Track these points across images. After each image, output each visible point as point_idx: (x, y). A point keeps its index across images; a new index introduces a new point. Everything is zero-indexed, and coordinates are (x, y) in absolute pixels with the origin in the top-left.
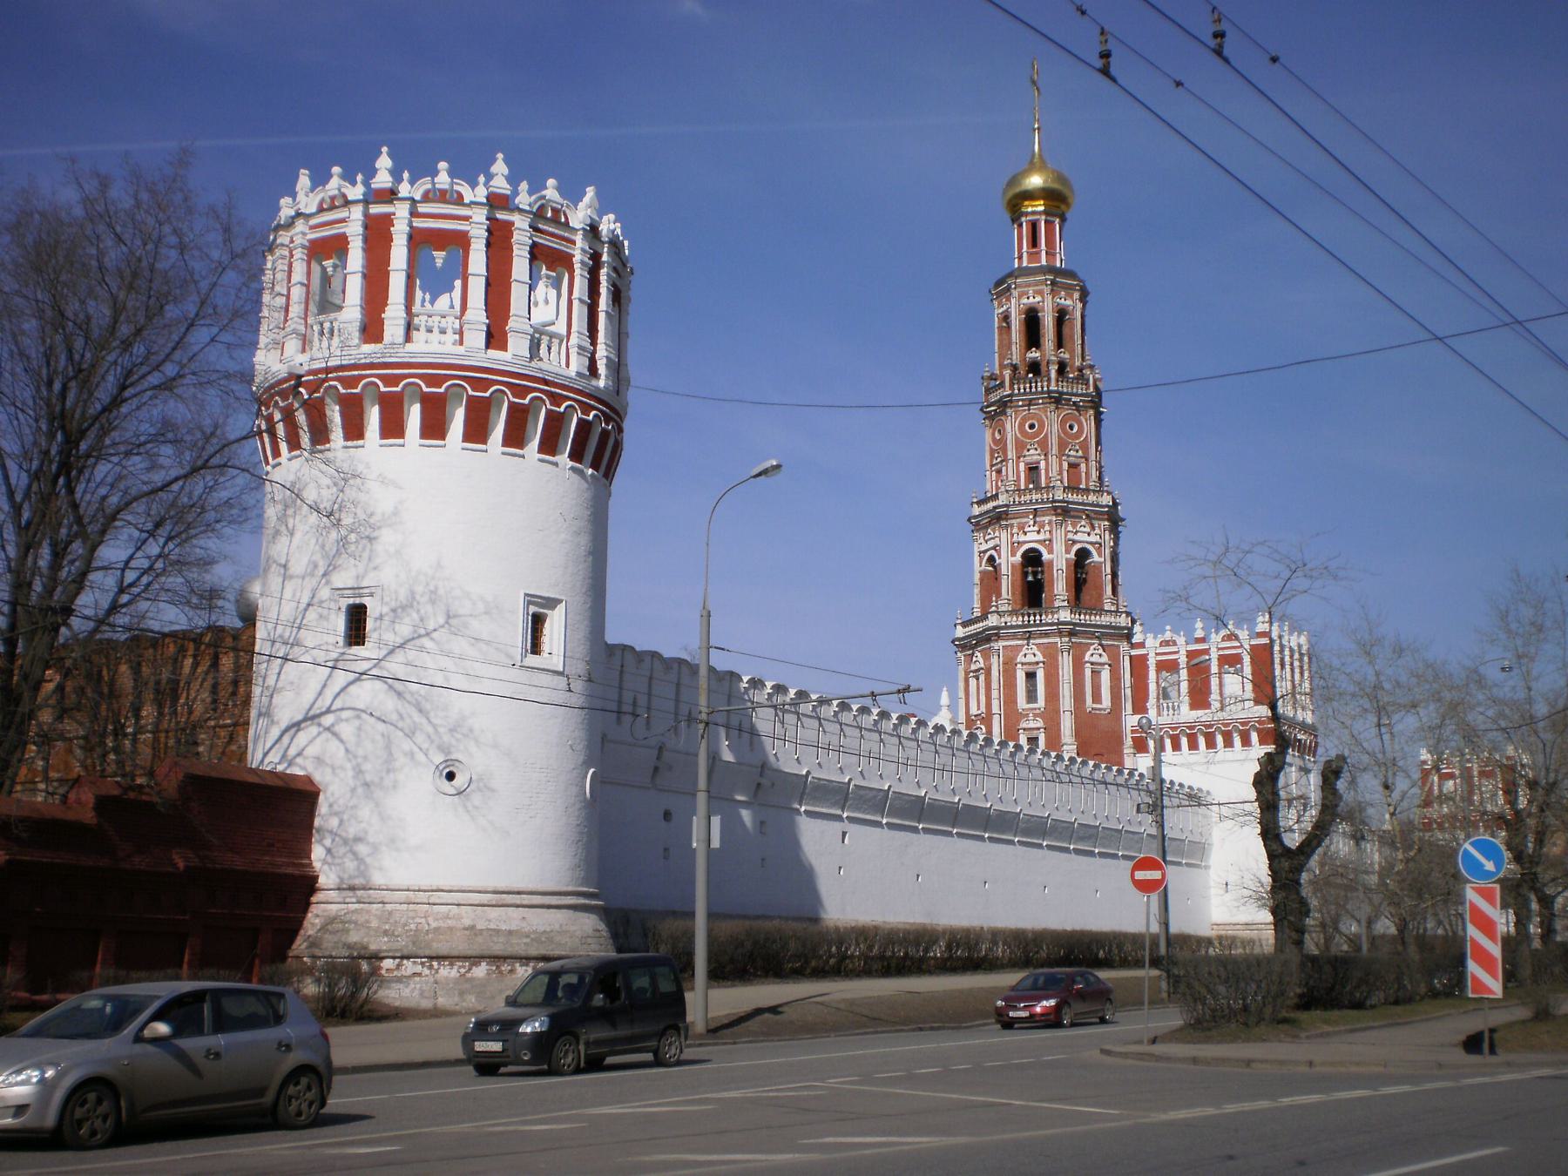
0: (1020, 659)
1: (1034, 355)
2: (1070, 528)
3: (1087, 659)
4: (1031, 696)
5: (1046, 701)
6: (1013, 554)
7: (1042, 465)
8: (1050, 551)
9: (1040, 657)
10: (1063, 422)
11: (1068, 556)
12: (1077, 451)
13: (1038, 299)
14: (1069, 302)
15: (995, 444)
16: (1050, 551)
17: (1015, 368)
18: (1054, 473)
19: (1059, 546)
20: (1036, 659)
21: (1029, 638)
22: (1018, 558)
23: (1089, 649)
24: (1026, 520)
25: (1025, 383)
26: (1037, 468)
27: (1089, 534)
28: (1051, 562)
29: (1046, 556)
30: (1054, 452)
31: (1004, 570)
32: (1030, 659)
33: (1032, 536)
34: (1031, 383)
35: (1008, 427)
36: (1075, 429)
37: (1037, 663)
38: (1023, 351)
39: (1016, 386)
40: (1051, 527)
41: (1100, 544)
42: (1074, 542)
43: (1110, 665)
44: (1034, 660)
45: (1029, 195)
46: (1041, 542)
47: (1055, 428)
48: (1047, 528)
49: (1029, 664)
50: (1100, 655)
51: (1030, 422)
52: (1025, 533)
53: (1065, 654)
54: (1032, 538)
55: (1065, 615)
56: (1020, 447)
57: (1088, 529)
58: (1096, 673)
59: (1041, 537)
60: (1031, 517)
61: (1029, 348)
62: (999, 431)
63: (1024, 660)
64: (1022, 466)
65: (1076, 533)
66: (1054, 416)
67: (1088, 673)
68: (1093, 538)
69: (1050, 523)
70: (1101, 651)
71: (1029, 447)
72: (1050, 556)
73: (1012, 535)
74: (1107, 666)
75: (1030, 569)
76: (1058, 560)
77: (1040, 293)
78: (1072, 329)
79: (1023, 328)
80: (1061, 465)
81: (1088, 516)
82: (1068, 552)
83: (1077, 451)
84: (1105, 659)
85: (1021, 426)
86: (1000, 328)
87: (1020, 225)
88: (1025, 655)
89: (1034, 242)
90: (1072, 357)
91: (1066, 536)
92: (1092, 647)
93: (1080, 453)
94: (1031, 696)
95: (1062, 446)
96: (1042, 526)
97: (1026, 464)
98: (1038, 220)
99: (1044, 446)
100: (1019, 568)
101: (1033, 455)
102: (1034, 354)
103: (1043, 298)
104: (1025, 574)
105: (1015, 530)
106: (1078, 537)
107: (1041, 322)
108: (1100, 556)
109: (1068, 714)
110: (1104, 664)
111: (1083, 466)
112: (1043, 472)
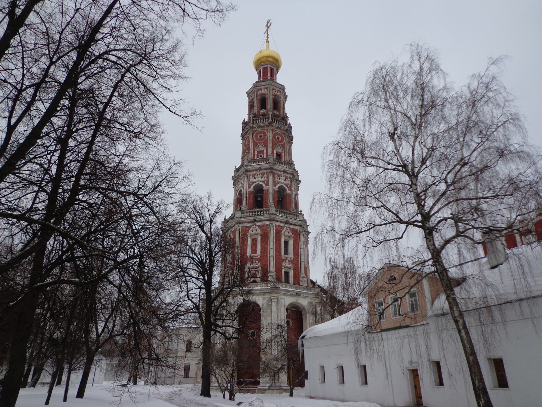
0: (250, 231)
3: (283, 232)
4: (254, 251)
5: (261, 252)
6: (250, 188)
9: (259, 231)
13: (266, 90)
14: (279, 93)
15: (245, 147)
16: (267, 184)
19: (271, 183)
20: (258, 232)
23: (283, 229)
28: (267, 190)
29: (265, 187)
32: (255, 232)
36: (280, 139)
38: (259, 110)
42: (278, 183)
44: (257, 232)
48: (265, 175)
52: (255, 178)
54: (259, 180)
55: (272, 210)
61: (261, 109)
64: (256, 152)
65: (279, 179)
70: (289, 230)
76: (271, 189)
77: (267, 88)
82: (275, 186)
85: (256, 136)
93: (282, 148)
94: (254, 251)
95: (274, 145)
99: (266, 144)
102: (263, 111)
105: (251, 177)
108: (290, 190)
110: (290, 237)
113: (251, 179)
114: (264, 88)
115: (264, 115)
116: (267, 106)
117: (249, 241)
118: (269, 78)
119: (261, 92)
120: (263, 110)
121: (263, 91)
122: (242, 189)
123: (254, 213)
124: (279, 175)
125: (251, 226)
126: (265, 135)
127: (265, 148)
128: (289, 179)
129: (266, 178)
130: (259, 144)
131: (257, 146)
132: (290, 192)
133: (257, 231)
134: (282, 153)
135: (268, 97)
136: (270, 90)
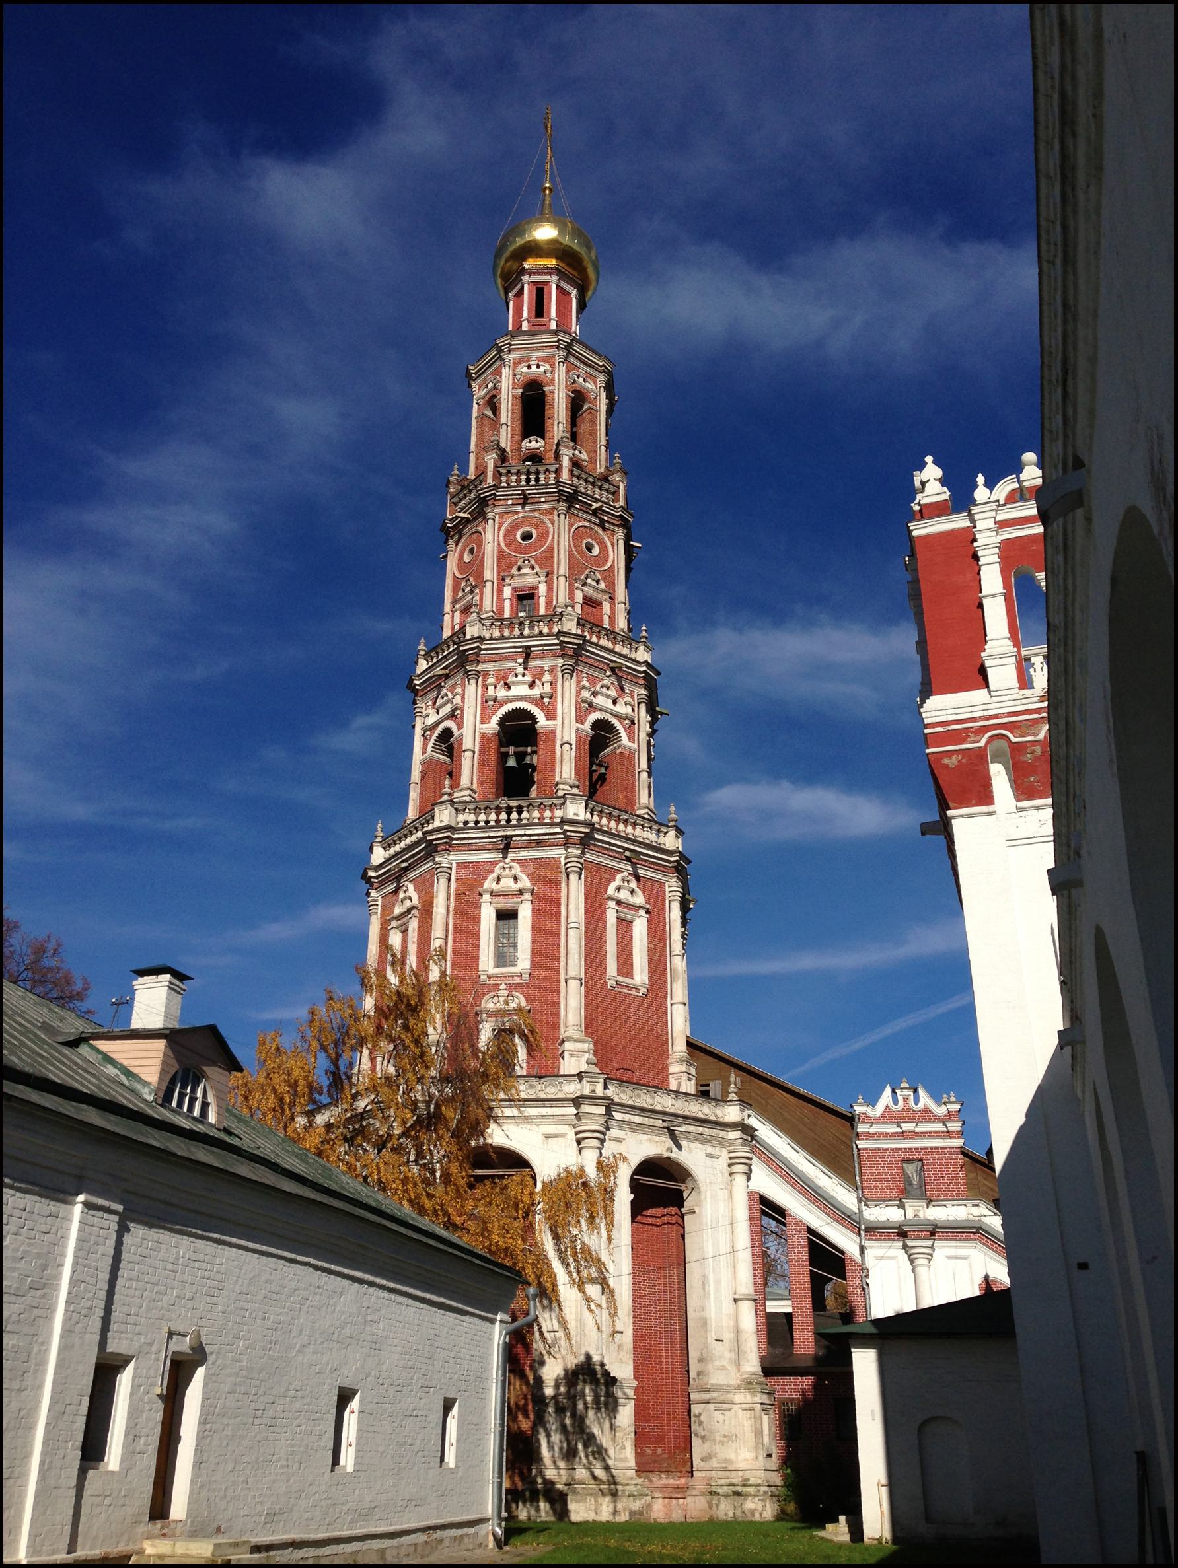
0: (489, 884)
1: (533, 444)
2: (585, 683)
3: (611, 890)
6: (485, 719)
7: (543, 589)
8: (551, 716)
9: (525, 883)
10: (577, 535)
11: (581, 726)
12: (598, 582)
14: (590, 385)
16: (551, 716)
17: (503, 457)
18: (562, 597)
19: (567, 706)
20: (519, 885)
21: (506, 850)
22: (494, 724)
24: (509, 665)
25: (518, 473)
26: (531, 596)
27: (615, 702)
28: (553, 733)
29: (542, 722)
30: (562, 572)
31: (467, 743)
32: (508, 884)
33: (520, 690)
34: (528, 473)
35: (488, 536)
36: (596, 551)
37: (521, 892)
38: (517, 437)
39: (504, 478)
40: (555, 676)
41: (633, 722)
43: (648, 912)
45: (534, 249)
46: (539, 701)
47: (565, 540)
48: (547, 677)
49: (506, 894)
50: (632, 892)
51: (524, 529)
52: (508, 686)
53: (573, 877)
55: (576, 810)
56: (505, 565)
57: (613, 693)
58: (624, 925)
59: (537, 691)
60: (520, 660)
61: (526, 434)
62: (472, 551)
63: (495, 887)
64: (507, 592)
65: (595, 694)
66: (564, 522)
67: (611, 917)
68: (622, 709)
69: (552, 670)
70: (633, 884)
71: (520, 563)
72: (551, 723)
73: (485, 688)
74: (642, 912)
75: (512, 749)
77: (549, 360)
78: (593, 422)
79: (518, 407)
80: (572, 596)
81: (613, 670)
82: (580, 719)
83: (598, 582)
84: (639, 899)
85: (510, 534)
86: (482, 417)
87: (520, 293)
88: (498, 879)
89: (540, 309)
90: (593, 460)
91: (578, 693)
92: (619, 877)
93: (602, 585)
96: (538, 675)
97: (514, 589)
98: (547, 283)
100: (494, 745)
101: (527, 578)
102: (534, 444)
103: (553, 367)
104: (504, 756)
105: (491, 680)
106: (599, 701)
107: (548, 400)
108: (632, 740)
109: (573, 984)
111: (606, 607)
112: (542, 601)
113: (491, 689)
114: (539, 358)
115: (535, 457)
116: (548, 425)
117: (487, 915)
118: (553, 326)
119: (525, 370)
120: (532, 438)
121: (534, 368)
122: (449, 724)
123: (504, 816)
124: (593, 680)
125: (494, 863)
126: (544, 532)
127: (543, 578)
128: (629, 699)
129: (547, 688)
130: (520, 563)
131: (514, 571)
132: (635, 746)
133: (516, 879)
134: (600, 604)
135: (552, 392)
136: (563, 368)
